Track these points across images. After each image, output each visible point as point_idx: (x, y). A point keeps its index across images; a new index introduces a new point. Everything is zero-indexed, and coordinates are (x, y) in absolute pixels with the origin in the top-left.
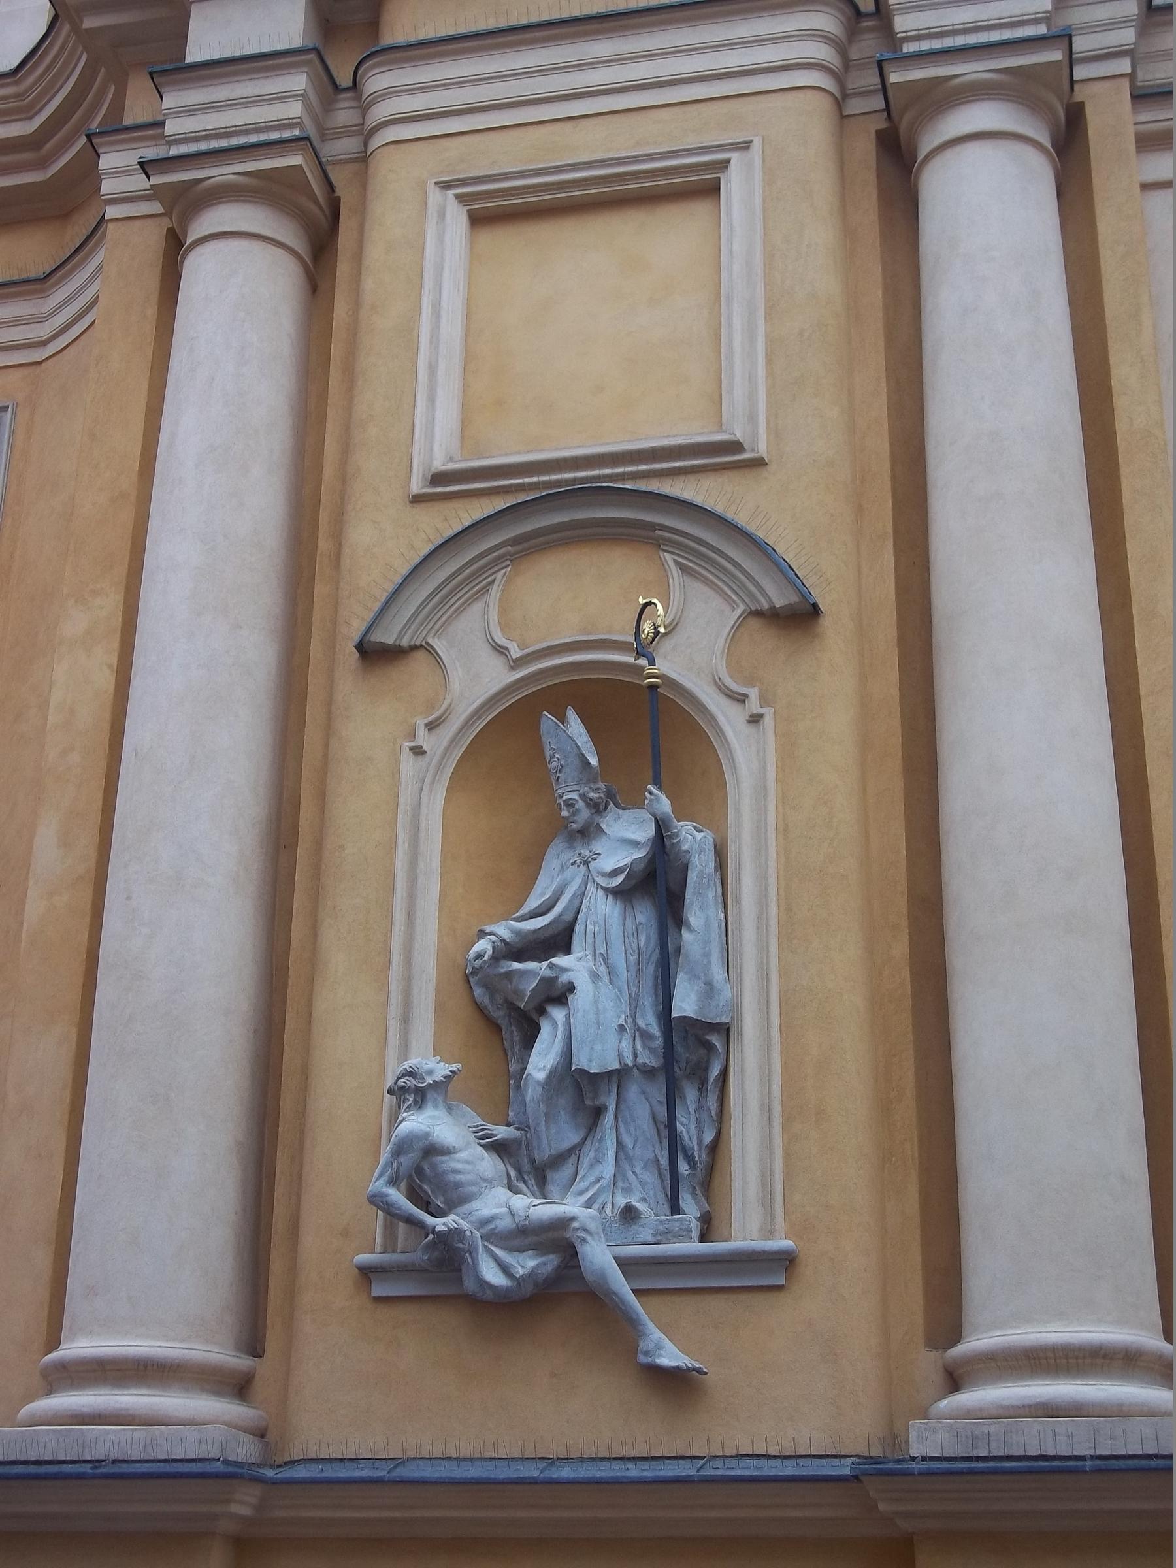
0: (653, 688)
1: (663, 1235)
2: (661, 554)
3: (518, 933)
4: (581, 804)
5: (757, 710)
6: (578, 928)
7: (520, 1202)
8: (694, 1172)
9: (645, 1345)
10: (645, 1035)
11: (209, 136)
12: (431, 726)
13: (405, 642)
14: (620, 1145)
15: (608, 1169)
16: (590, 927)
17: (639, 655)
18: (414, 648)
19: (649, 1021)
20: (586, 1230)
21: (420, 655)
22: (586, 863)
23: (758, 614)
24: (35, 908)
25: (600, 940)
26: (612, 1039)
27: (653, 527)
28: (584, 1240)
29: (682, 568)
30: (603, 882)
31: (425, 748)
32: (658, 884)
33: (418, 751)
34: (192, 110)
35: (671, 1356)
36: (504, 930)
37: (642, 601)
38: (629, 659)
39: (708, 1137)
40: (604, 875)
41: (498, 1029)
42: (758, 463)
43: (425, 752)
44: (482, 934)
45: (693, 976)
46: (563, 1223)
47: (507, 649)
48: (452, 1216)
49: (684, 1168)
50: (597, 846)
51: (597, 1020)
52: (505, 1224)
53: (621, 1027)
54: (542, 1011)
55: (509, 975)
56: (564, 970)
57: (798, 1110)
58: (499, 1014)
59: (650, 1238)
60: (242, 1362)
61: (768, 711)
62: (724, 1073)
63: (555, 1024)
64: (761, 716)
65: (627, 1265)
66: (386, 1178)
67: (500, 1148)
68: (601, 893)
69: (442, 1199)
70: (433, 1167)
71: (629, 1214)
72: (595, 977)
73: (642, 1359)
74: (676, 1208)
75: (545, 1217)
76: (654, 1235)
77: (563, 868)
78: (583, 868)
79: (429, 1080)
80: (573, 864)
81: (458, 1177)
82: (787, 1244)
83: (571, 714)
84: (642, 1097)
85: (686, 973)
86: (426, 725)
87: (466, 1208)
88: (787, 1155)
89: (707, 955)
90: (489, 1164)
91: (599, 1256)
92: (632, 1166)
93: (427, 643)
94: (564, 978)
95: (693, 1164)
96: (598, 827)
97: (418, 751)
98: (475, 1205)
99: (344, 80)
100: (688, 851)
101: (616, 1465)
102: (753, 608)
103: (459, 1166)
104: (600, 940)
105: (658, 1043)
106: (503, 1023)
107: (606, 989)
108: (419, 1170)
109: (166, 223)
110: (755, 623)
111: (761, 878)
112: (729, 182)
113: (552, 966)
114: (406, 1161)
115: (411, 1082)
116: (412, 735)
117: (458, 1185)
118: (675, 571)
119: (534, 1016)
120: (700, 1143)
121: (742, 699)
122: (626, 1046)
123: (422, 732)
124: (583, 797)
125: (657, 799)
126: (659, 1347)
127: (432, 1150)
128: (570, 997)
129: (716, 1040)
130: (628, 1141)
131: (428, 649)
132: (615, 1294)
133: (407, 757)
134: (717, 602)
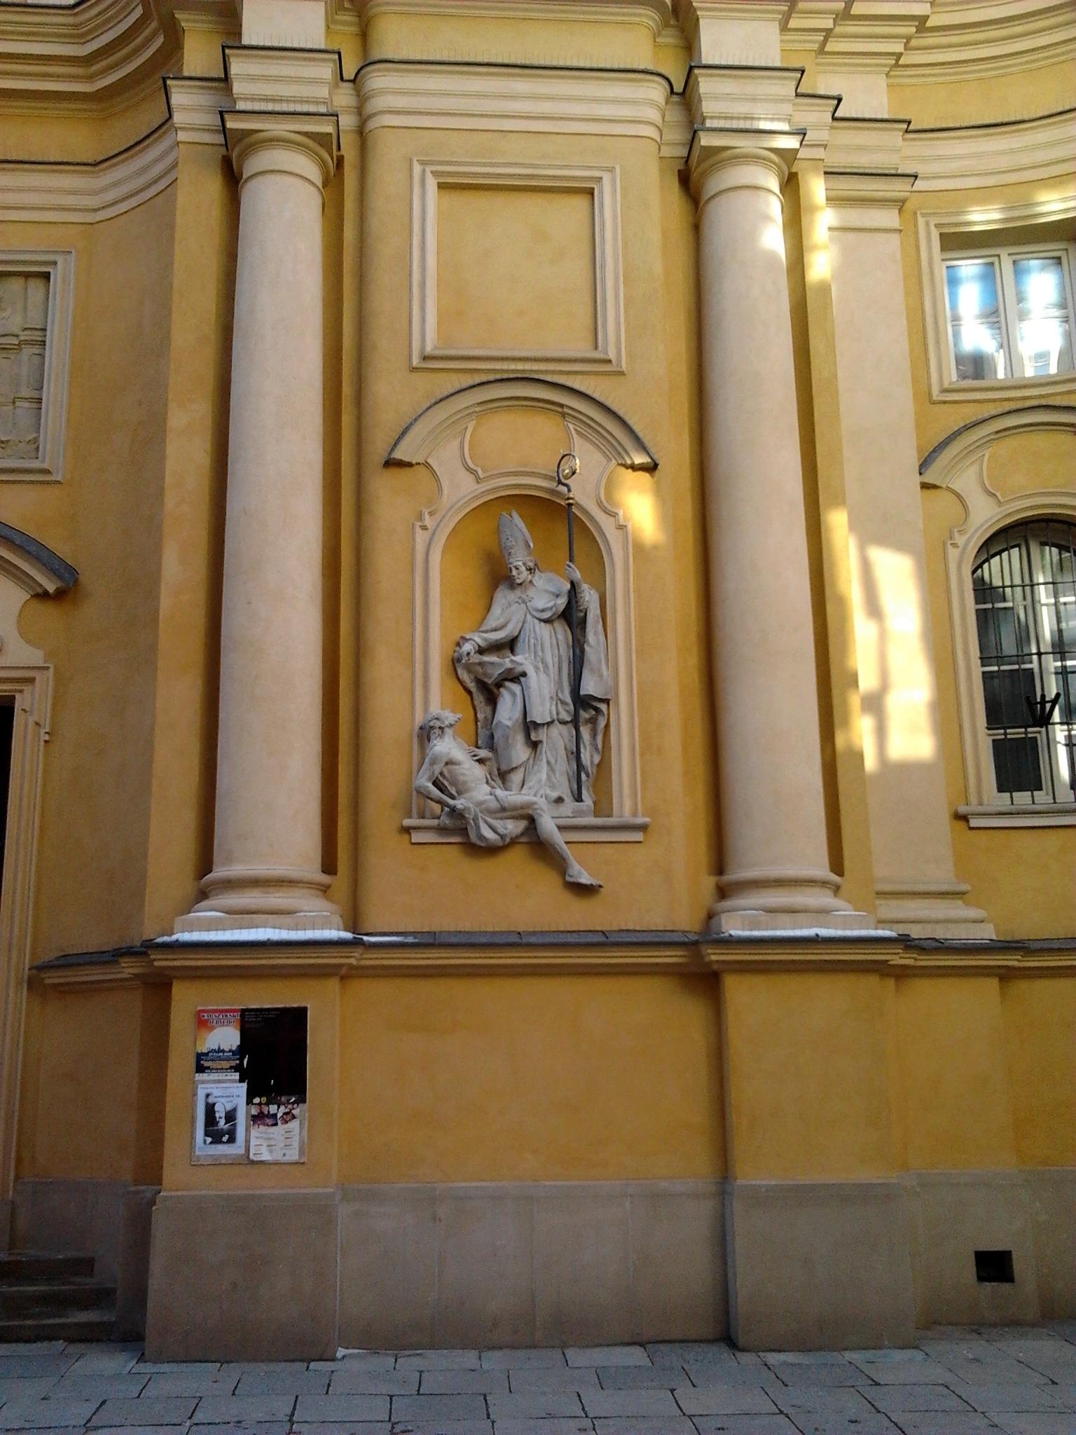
0: (570, 505)
3: (485, 640)
6: (521, 639)
7: (499, 792)
8: (588, 778)
9: (570, 871)
10: (563, 703)
11: (267, 99)
12: (431, 514)
14: (548, 762)
15: (544, 776)
17: (560, 482)
19: (568, 698)
21: (421, 468)
22: (524, 602)
24: (166, 603)
25: (539, 647)
26: (548, 704)
27: (562, 406)
29: (578, 433)
30: (538, 615)
32: (571, 616)
33: (424, 528)
34: (252, 78)
35: (585, 879)
36: (479, 639)
37: (562, 452)
38: (553, 485)
39: (597, 759)
40: (538, 610)
41: (469, 692)
42: (622, 373)
44: (466, 640)
45: (592, 670)
46: (529, 805)
48: (462, 801)
49: (583, 776)
50: (531, 592)
51: (543, 691)
52: (494, 805)
54: (499, 685)
55: (481, 664)
57: (648, 747)
58: (472, 686)
60: (325, 879)
62: (607, 726)
63: (514, 695)
66: (426, 777)
67: (481, 761)
70: (450, 772)
71: (559, 800)
72: (537, 668)
73: (568, 879)
74: (579, 799)
77: (510, 605)
78: (523, 606)
79: (447, 723)
81: (466, 778)
82: (647, 820)
83: (515, 514)
88: (643, 772)
89: (600, 661)
90: (479, 772)
91: (548, 825)
94: (519, 669)
95: (588, 776)
97: (424, 528)
98: (474, 794)
99: (349, 73)
101: (562, 936)
104: (539, 647)
105: (572, 707)
106: (474, 690)
107: (543, 676)
108: (441, 773)
109: (223, 151)
111: (628, 618)
112: (601, 192)
113: (512, 661)
114: (437, 768)
115: (438, 724)
117: (465, 782)
118: (575, 435)
120: (592, 762)
122: (554, 708)
123: (427, 516)
124: (524, 564)
126: (580, 873)
128: (522, 679)
129: (603, 707)
130: (552, 761)
131: (427, 465)
133: (418, 530)
134: (598, 456)
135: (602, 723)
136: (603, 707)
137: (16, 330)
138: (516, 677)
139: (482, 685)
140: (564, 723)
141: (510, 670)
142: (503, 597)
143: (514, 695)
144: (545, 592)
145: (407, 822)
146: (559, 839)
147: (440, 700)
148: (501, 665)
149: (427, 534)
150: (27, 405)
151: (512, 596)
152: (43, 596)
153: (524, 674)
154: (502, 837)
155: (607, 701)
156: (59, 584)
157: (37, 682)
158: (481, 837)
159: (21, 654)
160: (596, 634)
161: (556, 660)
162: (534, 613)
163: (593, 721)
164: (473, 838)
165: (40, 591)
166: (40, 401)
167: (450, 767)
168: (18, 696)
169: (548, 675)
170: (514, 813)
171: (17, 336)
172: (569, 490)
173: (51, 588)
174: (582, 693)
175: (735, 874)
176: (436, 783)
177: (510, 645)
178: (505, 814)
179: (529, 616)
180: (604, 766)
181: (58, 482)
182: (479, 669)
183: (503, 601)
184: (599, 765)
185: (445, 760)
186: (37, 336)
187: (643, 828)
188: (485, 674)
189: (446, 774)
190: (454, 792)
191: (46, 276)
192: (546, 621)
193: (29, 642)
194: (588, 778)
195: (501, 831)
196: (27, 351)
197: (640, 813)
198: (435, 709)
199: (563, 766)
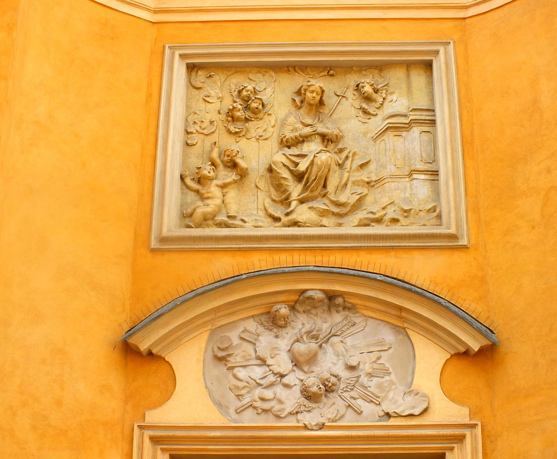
137: (403, 111)
150: (423, 177)
152: (466, 354)
156: (485, 342)
157: (468, 440)
159: (446, 411)
165: (462, 349)
166: (435, 173)
168: (448, 454)
171: (405, 116)
173: (475, 347)
181: (464, 248)
186: (424, 116)
191: (428, 66)
193: (453, 399)
196: (416, 130)
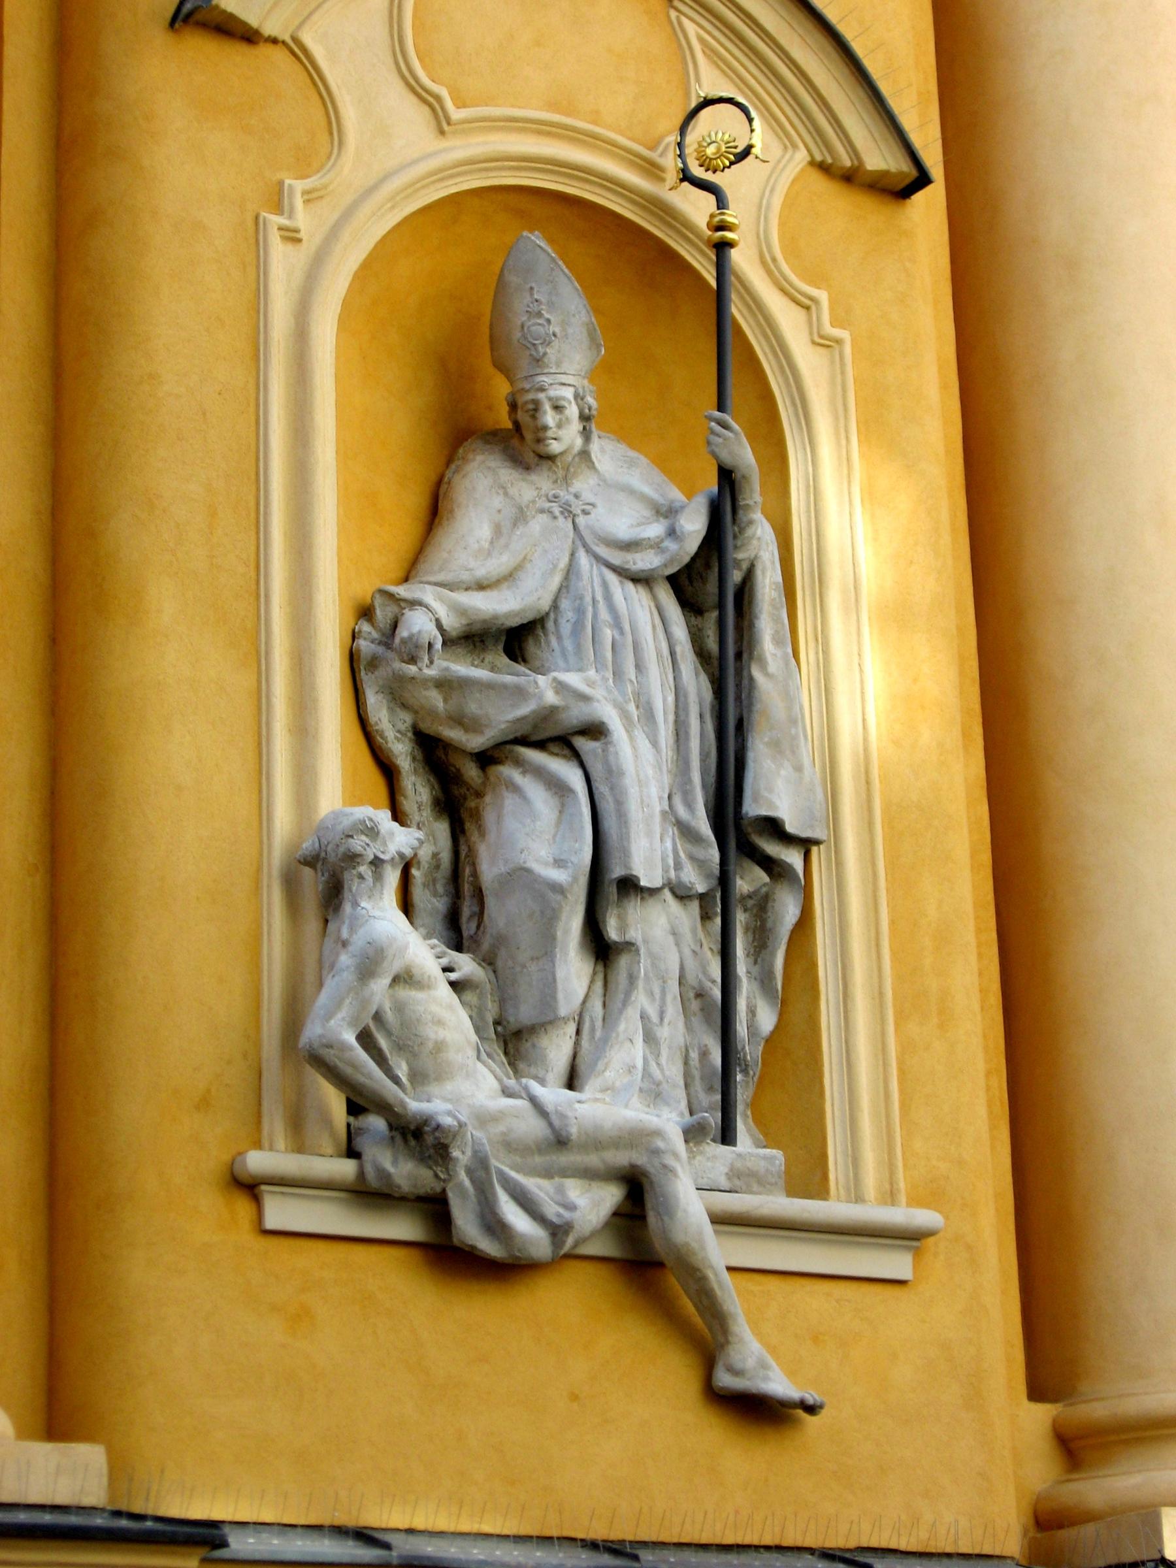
1: (741, 1179)
2: (673, 14)
3: (460, 611)
4: (573, 411)
5: (829, 330)
8: (751, 1077)
13: (268, 30)
14: (644, 1017)
16: (608, 634)
18: (274, 41)
20: (676, 1156)
21: (278, 55)
23: (824, 168)
28: (672, 1171)
30: (616, 558)
31: (302, 235)
33: (292, 236)
35: (779, 1385)
43: (299, 240)
46: (638, 1137)
47: (438, 98)
53: (664, 813)
56: (585, 698)
57: (913, 1000)
58: (401, 751)
59: (724, 1183)
61: (844, 334)
63: (559, 788)
64: (839, 342)
65: (722, 1220)
68: (612, 578)
69: (404, 1066)
70: (400, 1008)
73: (724, 1380)
74: (727, 1136)
75: (608, 1125)
76: (729, 1177)
77: (521, 517)
78: (565, 525)
80: (542, 511)
81: (442, 1034)
84: (671, 939)
85: (768, 744)
86: (305, 193)
87: (449, 1087)
88: (902, 1072)
91: (690, 1201)
92: (658, 1055)
93: (295, 40)
96: (585, 454)
97: (292, 236)
100: (759, 539)
102: (818, 158)
103: (434, 1008)
105: (715, 854)
110: (819, 182)
113: (561, 687)
116: (278, 200)
117: (440, 1047)
119: (471, 772)
121: (807, 305)
122: (669, 844)
123: (299, 202)
125: (740, 443)
126: (764, 1366)
127: (405, 978)
132: (712, 1267)
135: (788, 910)
136: (793, 858)
138: (566, 737)
139: (432, 750)
140: (682, 894)
141: (549, 714)
142: (487, 492)
143: (559, 788)
144: (630, 498)
145: (258, 1162)
146: (718, 1253)
147: (334, 789)
148: (520, 693)
149: (299, 257)
151: (530, 488)
153: (596, 731)
154: (557, 1231)
155: (806, 845)
158: (496, 1226)
160: (778, 642)
161: (671, 699)
162: (603, 551)
163: (762, 905)
164: (467, 1227)
167: (404, 993)
169: (655, 744)
170: (593, 1160)
172: (721, 203)
174: (752, 808)
175: (1108, 1400)
176: (365, 1038)
177: (517, 640)
178: (565, 1159)
179: (583, 560)
180: (796, 1043)
182: (435, 698)
183: (497, 501)
184: (771, 1041)
185: (396, 967)
187: (909, 1238)
188: (459, 720)
189: (390, 1016)
190: (402, 1071)
192: (642, 580)
194: (751, 1077)
195: (552, 1210)
197: (903, 1199)
198: (331, 798)
199: (673, 1030)
